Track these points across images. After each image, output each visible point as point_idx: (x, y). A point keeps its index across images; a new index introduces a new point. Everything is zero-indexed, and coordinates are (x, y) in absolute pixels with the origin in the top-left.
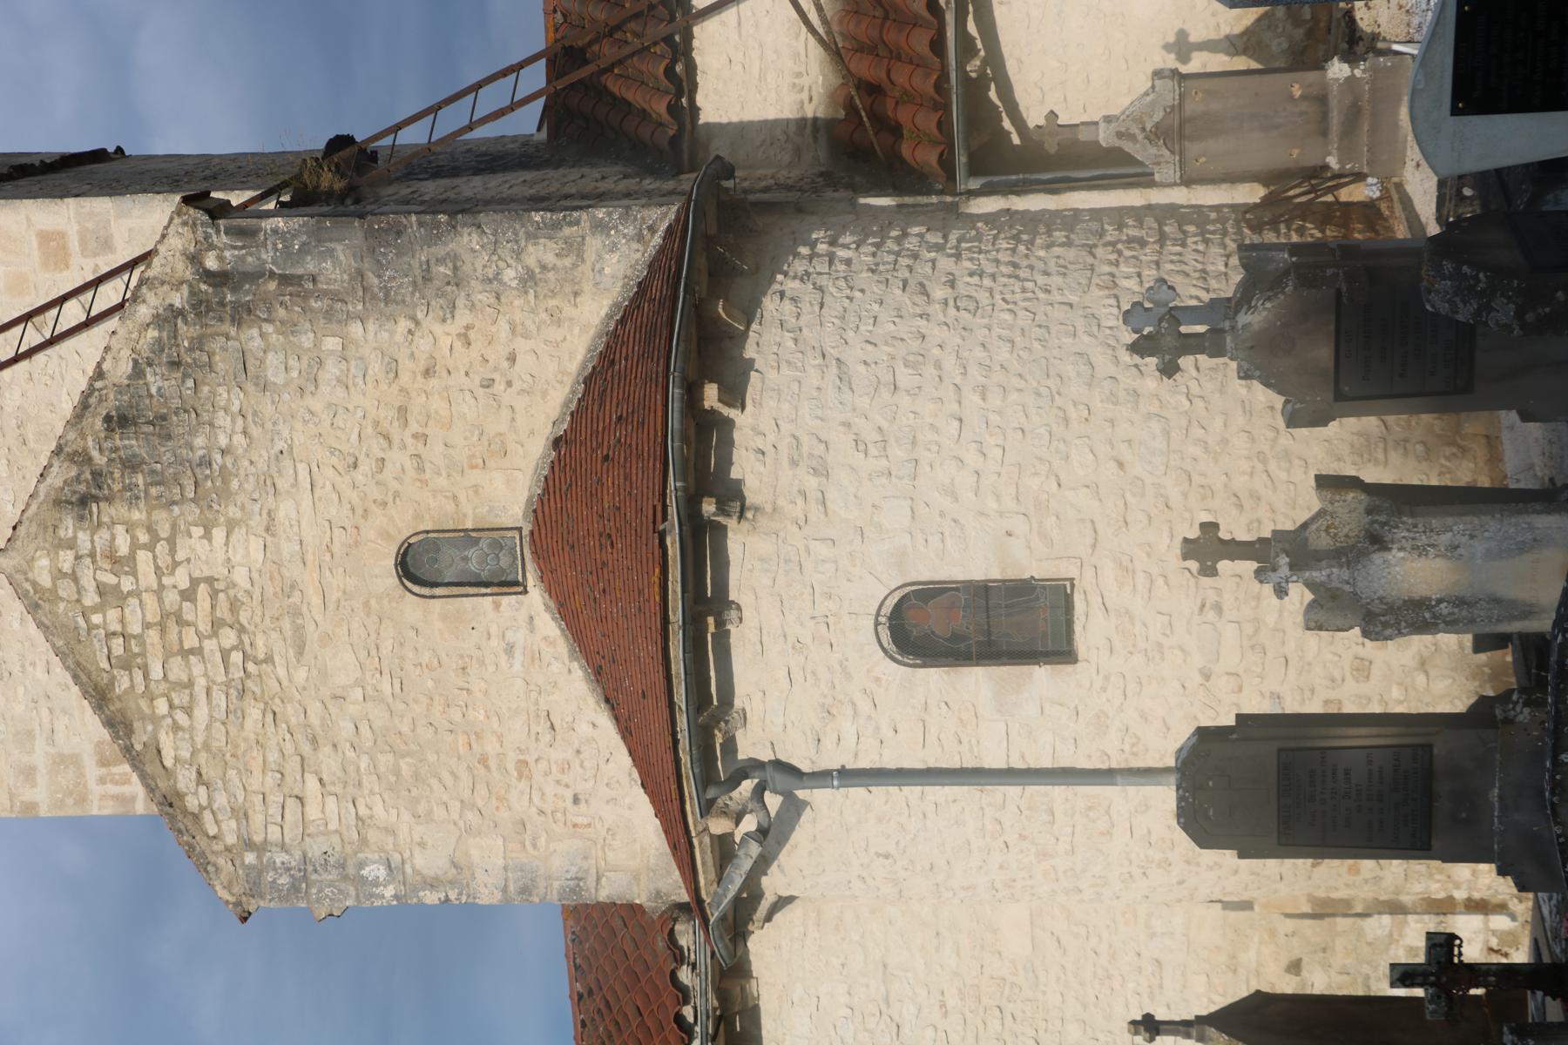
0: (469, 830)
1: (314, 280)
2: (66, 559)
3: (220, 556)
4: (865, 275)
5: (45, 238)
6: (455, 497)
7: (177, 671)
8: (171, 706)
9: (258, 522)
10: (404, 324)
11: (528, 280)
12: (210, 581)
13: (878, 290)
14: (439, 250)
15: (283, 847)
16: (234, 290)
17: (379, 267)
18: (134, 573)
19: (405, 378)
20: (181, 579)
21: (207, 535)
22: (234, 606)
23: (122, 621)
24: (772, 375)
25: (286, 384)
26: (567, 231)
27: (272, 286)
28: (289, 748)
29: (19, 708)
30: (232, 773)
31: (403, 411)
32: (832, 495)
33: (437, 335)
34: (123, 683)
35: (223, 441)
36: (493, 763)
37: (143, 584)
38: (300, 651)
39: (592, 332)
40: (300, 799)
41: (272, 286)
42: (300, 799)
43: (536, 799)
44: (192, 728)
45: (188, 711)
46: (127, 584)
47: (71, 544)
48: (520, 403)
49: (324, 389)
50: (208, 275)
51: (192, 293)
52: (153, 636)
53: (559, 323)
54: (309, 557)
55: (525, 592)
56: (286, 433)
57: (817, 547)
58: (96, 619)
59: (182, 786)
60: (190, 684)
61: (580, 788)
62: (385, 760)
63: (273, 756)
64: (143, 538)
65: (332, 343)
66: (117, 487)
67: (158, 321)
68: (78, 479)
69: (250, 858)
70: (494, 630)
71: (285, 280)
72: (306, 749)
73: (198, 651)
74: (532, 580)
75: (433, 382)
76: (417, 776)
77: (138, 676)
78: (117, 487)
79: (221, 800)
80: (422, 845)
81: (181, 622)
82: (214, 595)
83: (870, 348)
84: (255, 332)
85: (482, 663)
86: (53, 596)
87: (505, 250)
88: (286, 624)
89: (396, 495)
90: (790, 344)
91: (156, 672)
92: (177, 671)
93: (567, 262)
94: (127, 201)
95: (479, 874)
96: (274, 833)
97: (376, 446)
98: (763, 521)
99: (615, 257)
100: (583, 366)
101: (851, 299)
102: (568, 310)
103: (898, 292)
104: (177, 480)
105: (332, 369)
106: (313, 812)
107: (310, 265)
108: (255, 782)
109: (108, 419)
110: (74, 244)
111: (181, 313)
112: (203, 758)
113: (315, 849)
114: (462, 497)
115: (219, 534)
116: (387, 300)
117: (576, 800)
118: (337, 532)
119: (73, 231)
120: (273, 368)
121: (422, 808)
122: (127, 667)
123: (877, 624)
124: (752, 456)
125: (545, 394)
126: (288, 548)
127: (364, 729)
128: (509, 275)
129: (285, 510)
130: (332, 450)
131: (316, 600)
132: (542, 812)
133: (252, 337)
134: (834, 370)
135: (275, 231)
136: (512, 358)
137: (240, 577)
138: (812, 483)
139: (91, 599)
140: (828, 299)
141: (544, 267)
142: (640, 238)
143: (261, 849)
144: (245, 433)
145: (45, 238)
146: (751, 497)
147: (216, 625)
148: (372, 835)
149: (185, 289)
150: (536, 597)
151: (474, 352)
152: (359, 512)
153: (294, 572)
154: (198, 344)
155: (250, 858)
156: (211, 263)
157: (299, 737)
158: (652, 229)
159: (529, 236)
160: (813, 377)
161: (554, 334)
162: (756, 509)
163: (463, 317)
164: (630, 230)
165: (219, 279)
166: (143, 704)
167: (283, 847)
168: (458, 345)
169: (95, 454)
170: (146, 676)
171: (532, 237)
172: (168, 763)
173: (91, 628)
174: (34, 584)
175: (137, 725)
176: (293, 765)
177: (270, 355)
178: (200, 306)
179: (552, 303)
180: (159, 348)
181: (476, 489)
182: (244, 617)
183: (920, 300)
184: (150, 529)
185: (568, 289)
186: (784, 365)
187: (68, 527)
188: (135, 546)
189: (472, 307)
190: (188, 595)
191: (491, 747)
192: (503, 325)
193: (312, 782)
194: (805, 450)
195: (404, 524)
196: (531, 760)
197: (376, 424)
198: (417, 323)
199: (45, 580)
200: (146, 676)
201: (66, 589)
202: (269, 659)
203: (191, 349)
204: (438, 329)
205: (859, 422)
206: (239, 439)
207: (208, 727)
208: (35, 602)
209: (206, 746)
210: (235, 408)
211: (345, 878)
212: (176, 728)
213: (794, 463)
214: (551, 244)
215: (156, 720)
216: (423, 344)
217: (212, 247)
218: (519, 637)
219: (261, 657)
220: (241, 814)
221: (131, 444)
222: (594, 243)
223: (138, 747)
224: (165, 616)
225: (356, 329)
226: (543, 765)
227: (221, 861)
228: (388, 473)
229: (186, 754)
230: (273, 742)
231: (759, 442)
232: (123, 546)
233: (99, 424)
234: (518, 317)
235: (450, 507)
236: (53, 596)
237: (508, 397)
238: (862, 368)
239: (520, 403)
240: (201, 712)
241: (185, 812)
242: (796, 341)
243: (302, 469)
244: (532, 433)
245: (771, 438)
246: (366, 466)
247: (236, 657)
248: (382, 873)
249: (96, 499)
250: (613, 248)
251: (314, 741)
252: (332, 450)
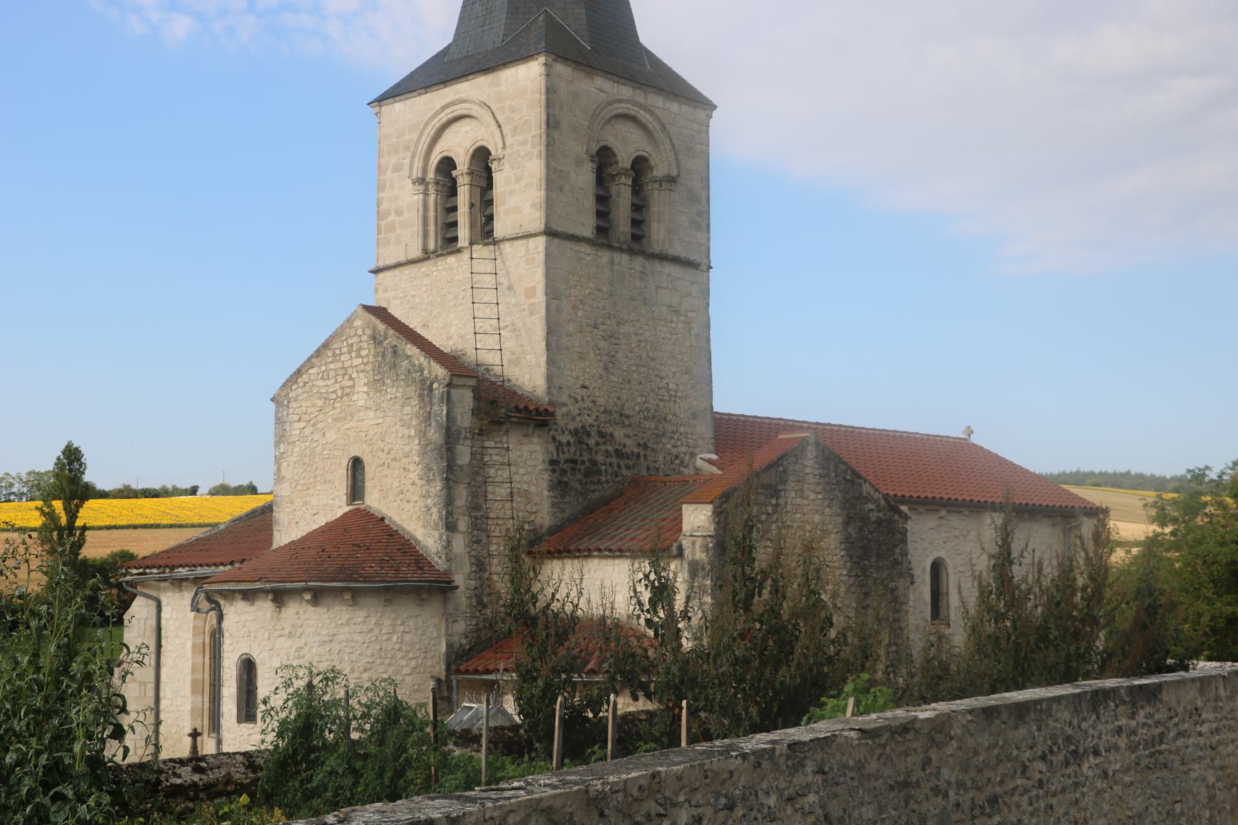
0: (291, 483)
1: (430, 425)
2: (360, 332)
3: (360, 389)
4: (378, 647)
5: (533, 289)
6: (373, 479)
7: (332, 374)
8: (324, 372)
9: (369, 403)
10: (417, 459)
11: (428, 509)
12: (354, 386)
13: (369, 653)
14: (437, 474)
15: (288, 415)
16: (428, 394)
17: (431, 451)
18: (356, 357)
19: (404, 460)
20: (355, 375)
21: (365, 385)
22: (348, 395)
23: (344, 353)
24: (326, 617)
25: (403, 414)
26: (441, 524)
27: (428, 409)
28: (312, 416)
29: (403, 285)
30: (306, 395)
31: (394, 459)
32: (283, 639)
33: (415, 473)
34: (330, 353)
35: (389, 390)
36: (306, 492)
37: (354, 360)
38: (336, 420)
39: (413, 533)
40: (299, 420)
41: (428, 409)
42: (299, 420)
43: (298, 508)
44: (317, 379)
45: (322, 378)
46: (353, 354)
47: (364, 333)
48: (396, 504)
49: (401, 429)
50: (432, 384)
51: (427, 378)
52: (340, 365)
53: (417, 520)
54: (359, 423)
55: (348, 505)
56: (391, 414)
57: (267, 633)
58: (345, 343)
59: (304, 376)
60: (329, 379)
61: (300, 524)
62: (308, 451)
63: (309, 410)
64: (365, 360)
65: (413, 432)
66: (378, 350)
67: (420, 365)
68: (380, 335)
69: (286, 402)
70: (339, 493)
71: (430, 413)
72: (312, 422)
73: (336, 382)
74: (351, 508)
75: (402, 470)
76: (304, 464)
77: (330, 360)
78: (378, 350)
79: (300, 391)
80: (288, 465)
81: (344, 374)
82: (350, 387)
83: (337, 651)
84: (416, 402)
85: (331, 488)
86: (351, 327)
87: (436, 500)
88: (343, 415)
89: (374, 456)
90: (340, 622)
91: (332, 366)
92: (332, 374)
93: (432, 524)
94: (544, 322)
95: (280, 486)
96: (291, 411)
97: (386, 450)
98: (276, 614)
99: (432, 542)
100: (403, 529)
101: (364, 642)
102: (420, 523)
103: (366, 661)
104: (379, 373)
105: (406, 432)
106: (296, 425)
107: (433, 424)
108: (304, 404)
109: (396, 346)
110: (532, 301)
111: (422, 374)
112: (311, 384)
113: (287, 426)
114: (373, 482)
115: (365, 389)
116: (424, 453)
117: (297, 523)
118: (365, 434)
119: (536, 300)
120: (408, 409)
121: (297, 466)
122: (334, 355)
123: (247, 654)
124: (296, 610)
125: (398, 514)
126: (361, 414)
127: (316, 444)
128: (429, 501)
129: (371, 414)
130: (386, 432)
131: (348, 426)
132: (295, 510)
133: (415, 402)
134: (327, 639)
135: (442, 410)
136: (408, 501)
137: (355, 397)
138: (287, 632)
139: (350, 341)
140: (364, 635)
141: (431, 515)
142: (438, 552)
143: (288, 406)
144: (391, 398)
145: (533, 289)
146: (283, 610)
147: (342, 388)
148: (291, 447)
149: (428, 375)
150: (347, 509)
151: (410, 487)
152: (371, 442)
153: (356, 418)
154: (414, 381)
155: (286, 402)
156: (435, 385)
157: (314, 420)
158: (440, 557)
159: (439, 509)
160: (324, 632)
161: (414, 518)
162: (280, 612)
163: (419, 483)
164: (440, 549)
165: (431, 390)
166: (323, 362)
167: (288, 415)
168: (412, 481)
169: (387, 341)
170: (331, 362)
171: (439, 511)
172: (310, 371)
173: (343, 341)
174: (354, 320)
175: (319, 359)
176: (306, 417)
177: (410, 408)
178: (423, 381)
179: (422, 517)
180: (414, 366)
181: (375, 486)
182: (345, 398)
183: (361, 669)
184: (367, 362)
185: (425, 524)
186: (329, 621)
187: (368, 332)
188: (363, 357)
189: (422, 487)
190: (351, 378)
191: (311, 492)
192: (415, 498)
193: (303, 424)
194: (298, 629)
195: (367, 460)
196: (307, 506)
197: (392, 448)
198: (418, 465)
199: (355, 324)
200: (331, 362)
201: (352, 332)
202: (334, 408)
203: (412, 378)
204: (416, 473)
205: (307, 649)
206: (389, 396)
207: (317, 386)
208: (349, 321)
209: (313, 385)
210: (398, 395)
211: (280, 437)
212: (318, 374)
213: (293, 626)
214: (437, 518)
215: (320, 367)
216: (412, 467)
217: (439, 385)
218: (337, 502)
219: (335, 405)
220: (296, 399)
221: (389, 355)
222: (436, 534)
223: (313, 360)
224: (345, 369)
225: (417, 442)
226: (306, 511)
227: (285, 391)
228: (381, 454)
229: (312, 378)
230: (313, 410)
231: (301, 612)
232: (364, 353)
233: (394, 343)
234: (419, 504)
235: (371, 477)
236: (351, 327)
237: (398, 499)
238: (328, 649)
239: (396, 504)
240: (320, 383)
241: (297, 378)
242: (342, 624)
243: (381, 421)
244: (388, 508)
245: (302, 617)
246: (381, 444)
247: (334, 396)
248: (282, 451)
249: (375, 342)
250: (435, 542)
251: (314, 425)
252: (386, 432)
